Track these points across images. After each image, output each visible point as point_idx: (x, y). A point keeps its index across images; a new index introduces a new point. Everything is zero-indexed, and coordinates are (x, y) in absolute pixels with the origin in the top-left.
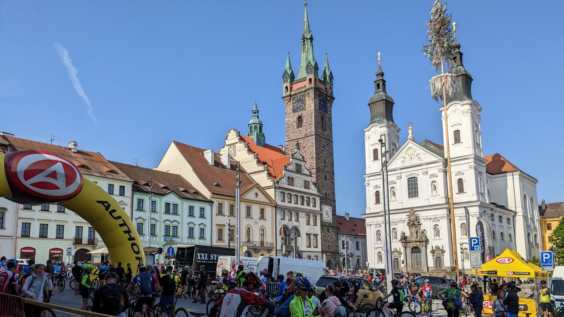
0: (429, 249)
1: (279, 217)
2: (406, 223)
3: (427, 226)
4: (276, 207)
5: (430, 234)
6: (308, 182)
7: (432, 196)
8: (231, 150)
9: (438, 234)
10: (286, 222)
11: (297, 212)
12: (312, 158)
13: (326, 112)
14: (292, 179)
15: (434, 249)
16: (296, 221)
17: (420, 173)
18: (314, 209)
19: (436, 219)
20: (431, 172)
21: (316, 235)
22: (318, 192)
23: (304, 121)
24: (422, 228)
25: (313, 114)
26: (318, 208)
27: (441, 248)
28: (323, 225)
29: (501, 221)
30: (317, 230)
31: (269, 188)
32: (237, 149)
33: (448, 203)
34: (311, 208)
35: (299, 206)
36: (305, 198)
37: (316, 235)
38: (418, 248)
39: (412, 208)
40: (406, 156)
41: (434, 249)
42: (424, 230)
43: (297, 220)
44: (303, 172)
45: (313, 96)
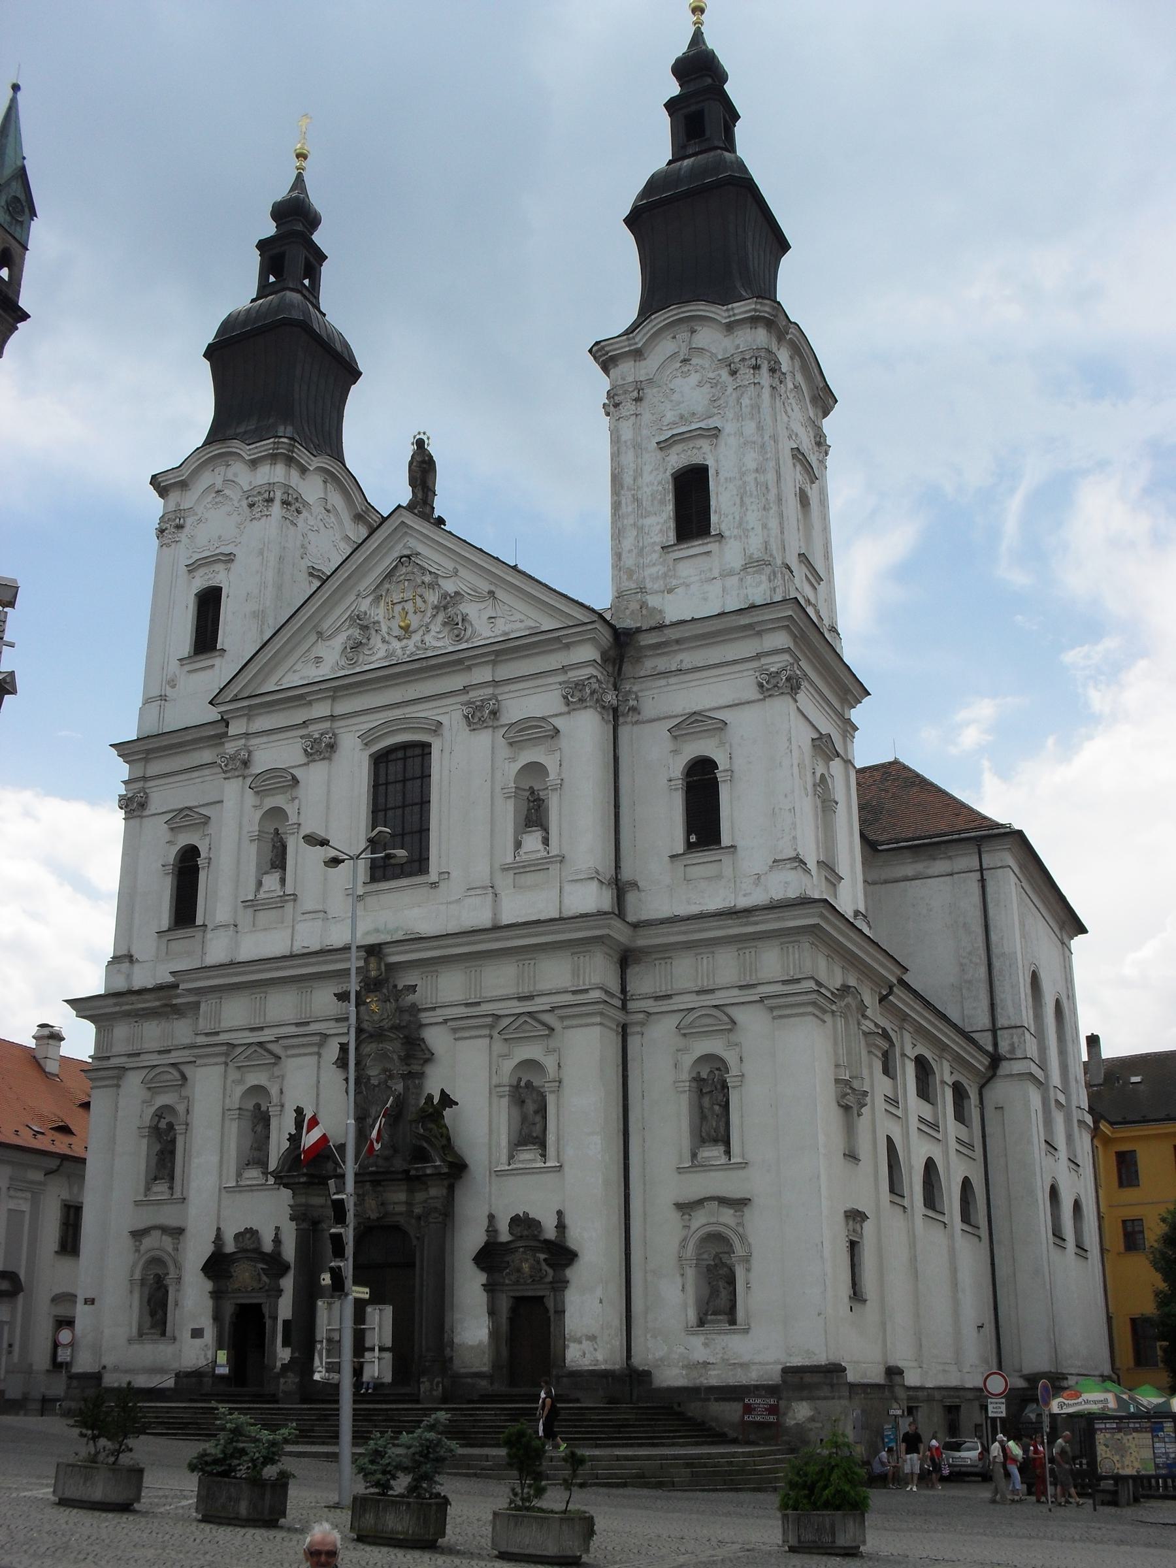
0: (470, 1238)
2: (332, 1051)
3: (468, 1078)
5: (480, 1124)
7: (519, 869)
9: (531, 1127)
15: (504, 1236)
17: (452, 717)
19: (536, 1022)
20: (520, 706)
24: (434, 1085)
29: (925, 1092)
33: (619, 910)
38: (397, 1228)
39: (373, 951)
40: (379, 613)
41: (504, 1236)
42: (447, 1101)
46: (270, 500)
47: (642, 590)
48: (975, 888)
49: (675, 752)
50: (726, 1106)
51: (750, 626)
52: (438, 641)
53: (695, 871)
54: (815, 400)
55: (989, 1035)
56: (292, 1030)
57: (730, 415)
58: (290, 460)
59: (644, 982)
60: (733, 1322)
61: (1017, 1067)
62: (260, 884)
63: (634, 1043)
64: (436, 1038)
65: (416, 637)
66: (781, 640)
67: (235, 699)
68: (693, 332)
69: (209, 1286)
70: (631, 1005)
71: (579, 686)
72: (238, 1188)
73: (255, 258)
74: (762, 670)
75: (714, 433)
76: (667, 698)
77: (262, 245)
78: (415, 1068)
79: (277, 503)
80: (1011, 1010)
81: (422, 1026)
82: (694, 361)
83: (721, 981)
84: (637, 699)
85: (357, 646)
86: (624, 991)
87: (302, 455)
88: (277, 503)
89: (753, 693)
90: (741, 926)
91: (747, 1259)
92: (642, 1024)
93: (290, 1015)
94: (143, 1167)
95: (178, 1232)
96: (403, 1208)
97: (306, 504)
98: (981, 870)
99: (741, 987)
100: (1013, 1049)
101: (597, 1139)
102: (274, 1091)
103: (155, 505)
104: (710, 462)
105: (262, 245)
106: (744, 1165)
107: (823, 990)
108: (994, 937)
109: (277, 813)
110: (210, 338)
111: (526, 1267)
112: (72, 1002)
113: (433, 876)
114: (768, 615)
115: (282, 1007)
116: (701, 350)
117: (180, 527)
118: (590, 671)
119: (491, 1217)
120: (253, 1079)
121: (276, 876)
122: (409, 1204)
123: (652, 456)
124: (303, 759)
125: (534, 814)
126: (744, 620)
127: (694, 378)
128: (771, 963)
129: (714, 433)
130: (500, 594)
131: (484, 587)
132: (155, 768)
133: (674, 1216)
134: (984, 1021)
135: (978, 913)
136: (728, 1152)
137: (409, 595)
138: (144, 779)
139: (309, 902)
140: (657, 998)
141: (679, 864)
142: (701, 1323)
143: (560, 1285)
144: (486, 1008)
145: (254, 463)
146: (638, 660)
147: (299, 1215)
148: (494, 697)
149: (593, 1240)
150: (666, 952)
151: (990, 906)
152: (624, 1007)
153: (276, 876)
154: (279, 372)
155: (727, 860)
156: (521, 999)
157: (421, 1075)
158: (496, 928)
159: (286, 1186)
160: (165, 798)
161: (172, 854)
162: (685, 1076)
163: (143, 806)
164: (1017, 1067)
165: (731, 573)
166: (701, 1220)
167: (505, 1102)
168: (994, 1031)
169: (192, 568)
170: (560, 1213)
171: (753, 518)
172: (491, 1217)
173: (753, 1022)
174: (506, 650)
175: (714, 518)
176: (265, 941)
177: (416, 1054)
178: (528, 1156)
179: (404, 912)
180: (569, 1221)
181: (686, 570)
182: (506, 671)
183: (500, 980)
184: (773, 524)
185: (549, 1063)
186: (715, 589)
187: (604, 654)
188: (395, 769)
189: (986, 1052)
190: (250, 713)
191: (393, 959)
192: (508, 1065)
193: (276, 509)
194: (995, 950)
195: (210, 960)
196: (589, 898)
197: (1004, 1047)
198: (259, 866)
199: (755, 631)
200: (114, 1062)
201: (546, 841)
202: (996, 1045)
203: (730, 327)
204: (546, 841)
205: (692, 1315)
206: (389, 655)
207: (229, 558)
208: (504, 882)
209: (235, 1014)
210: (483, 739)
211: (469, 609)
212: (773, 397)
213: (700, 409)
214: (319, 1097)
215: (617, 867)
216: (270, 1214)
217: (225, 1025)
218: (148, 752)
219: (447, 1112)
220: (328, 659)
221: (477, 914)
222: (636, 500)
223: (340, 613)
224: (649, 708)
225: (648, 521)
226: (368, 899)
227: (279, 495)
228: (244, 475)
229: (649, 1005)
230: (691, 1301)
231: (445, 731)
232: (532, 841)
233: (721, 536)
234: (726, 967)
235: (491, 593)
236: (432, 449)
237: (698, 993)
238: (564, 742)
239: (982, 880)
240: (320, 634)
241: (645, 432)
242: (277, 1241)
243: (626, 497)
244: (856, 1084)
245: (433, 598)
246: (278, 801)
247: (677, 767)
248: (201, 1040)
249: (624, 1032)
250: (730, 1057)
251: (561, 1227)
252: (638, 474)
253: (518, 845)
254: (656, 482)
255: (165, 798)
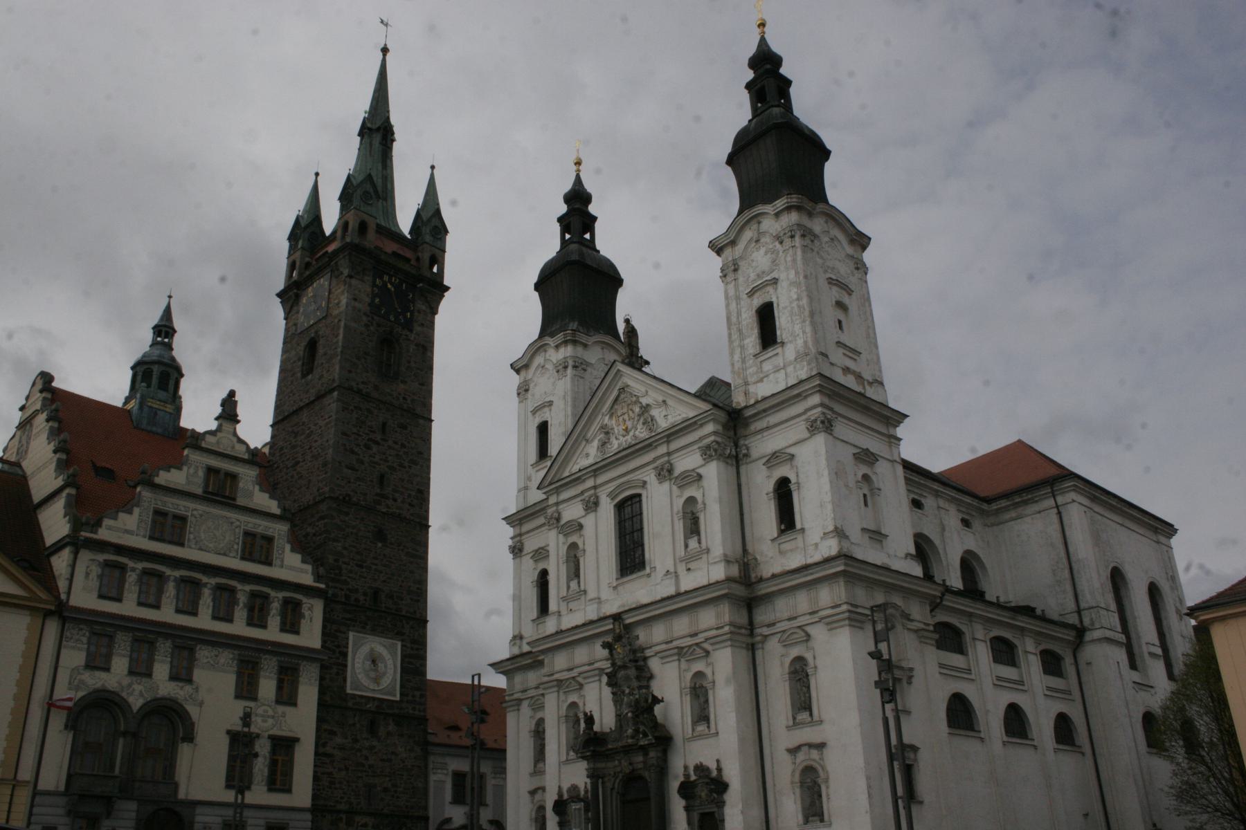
1: (74, 657)
3: (669, 683)
4: (62, 613)
6: (269, 540)
7: (690, 559)
8: (24, 438)
10: (117, 675)
11: (186, 644)
12: (325, 464)
13: (408, 325)
14: (183, 519)
16: (174, 677)
17: (650, 476)
18: (288, 639)
21: (284, 745)
22: (318, 578)
23: (321, 351)
25: (342, 324)
26: (311, 636)
27: (715, 773)
28: (334, 704)
30: (302, 720)
31: (58, 547)
32: (34, 431)
34: (273, 633)
35: (204, 621)
36: (242, 599)
37: (284, 745)
39: (617, 617)
42: (656, 700)
43: (182, 675)
44: (241, 501)
45: (346, 272)
46: (566, 367)
47: (746, 384)
48: (1055, 518)
49: (768, 477)
50: (808, 688)
51: (798, 395)
52: (642, 433)
53: (785, 547)
54: (852, 242)
55: (1076, 615)
56: (586, 668)
57: (782, 268)
58: (575, 342)
59: (762, 616)
60: (822, 820)
61: (1097, 634)
62: (568, 587)
63: (759, 653)
64: (654, 664)
65: (631, 434)
66: (816, 399)
67: (551, 484)
68: (759, 223)
69: (557, 819)
70: (758, 631)
71: (708, 447)
72: (568, 761)
73: (557, 228)
74: (807, 420)
75: (775, 281)
76: (762, 445)
77: (560, 220)
78: (645, 683)
79: (570, 368)
80: (1088, 596)
81: (645, 659)
82: (762, 240)
83: (800, 611)
84: (748, 449)
85: (604, 444)
86: (751, 623)
87: (583, 338)
88: (570, 368)
89: (807, 435)
90: (807, 577)
91: (827, 780)
92: (763, 642)
93: (585, 659)
94: (532, 754)
95: (543, 789)
96: (640, 766)
97: (588, 364)
98: (1057, 507)
99: (810, 614)
100: (1093, 624)
101: (733, 715)
102: (581, 705)
103: (515, 379)
104: (774, 299)
105: (560, 220)
106: (821, 722)
107: (860, 610)
108: (1071, 550)
109: (574, 546)
110: (535, 279)
111: (703, 794)
112: (492, 665)
113: (648, 570)
114: (807, 386)
115: (581, 655)
116: (764, 233)
117: (527, 390)
118: (712, 438)
119: (686, 768)
120: (573, 698)
121: (576, 581)
122: (644, 762)
123: (745, 301)
124: (583, 513)
125: (693, 526)
126: (796, 392)
127: (762, 251)
128: (827, 596)
129: (775, 281)
130: (669, 402)
131: (660, 399)
132: (526, 528)
133: (787, 757)
134: (1071, 606)
135: (1059, 535)
136: (811, 715)
137: (625, 410)
138: (520, 535)
139: (592, 594)
140: (769, 626)
141: (776, 544)
142: (806, 821)
143: (721, 804)
144: (675, 644)
145: (557, 347)
146: (747, 425)
147: (594, 775)
148: (669, 462)
149: (733, 774)
150: (769, 597)
151: (1066, 529)
152: (752, 634)
153: (576, 581)
154: (579, 289)
155: (800, 537)
156: (691, 636)
157: (648, 687)
158: (678, 595)
159: (583, 758)
160: (531, 544)
161: (537, 573)
162: (787, 670)
163: (521, 550)
164: (1097, 634)
165: (790, 363)
166: (801, 756)
167: (688, 698)
168: (1079, 612)
169: (534, 412)
170: (718, 761)
171: (797, 328)
172: (686, 768)
173: (818, 632)
174: (672, 434)
175: (778, 333)
176: (571, 620)
177: (644, 675)
178: (701, 728)
179: (640, 591)
180: (723, 766)
181: (767, 367)
182: (674, 445)
183: (681, 625)
184: (808, 329)
185: (708, 671)
186: (782, 374)
187: (725, 426)
188: (628, 510)
189: (1071, 627)
190: (557, 491)
191: (628, 621)
192: (689, 675)
193: (569, 371)
194: (1073, 559)
195: (548, 633)
196: (718, 572)
197: (1086, 621)
198: (568, 577)
199: (800, 397)
200: (516, 696)
201: (699, 542)
202: (1081, 622)
203: (777, 215)
204: (699, 542)
205: (800, 817)
206: (619, 445)
207: (550, 403)
208: (681, 569)
209: (560, 662)
210: (666, 485)
211: (655, 412)
212: (804, 252)
213: (767, 269)
214: (600, 705)
215: (745, 550)
216: (578, 775)
217: (557, 668)
218: (520, 520)
219: (658, 709)
220: (590, 454)
221: (668, 589)
222: (740, 331)
223: (595, 426)
224: (755, 453)
225: (746, 341)
226: (620, 588)
227: (571, 363)
228: (557, 354)
229: (765, 631)
230: (800, 809)
231: (648, 486)
232: (693, 543)
233: (783, 343)
234: (801, 602)
235: (664, 401)
236: (634, 323)
237: (789, 619)
238: (705, 482)
239: (1059, 513)
240: (587, 441)
241: (741, 288)
242: (586, 792)
243: (734, 328)
244: (904, 664)
245: (637, 410)
246: (574, 538)
247: (770, 486)
248: (546, 679)
249: (752, 648)
250: (808, 656)
251: (719, 770)
252: (739, 314)
253: (686, 546)
254: (749, 319)
255: (531, 544)
